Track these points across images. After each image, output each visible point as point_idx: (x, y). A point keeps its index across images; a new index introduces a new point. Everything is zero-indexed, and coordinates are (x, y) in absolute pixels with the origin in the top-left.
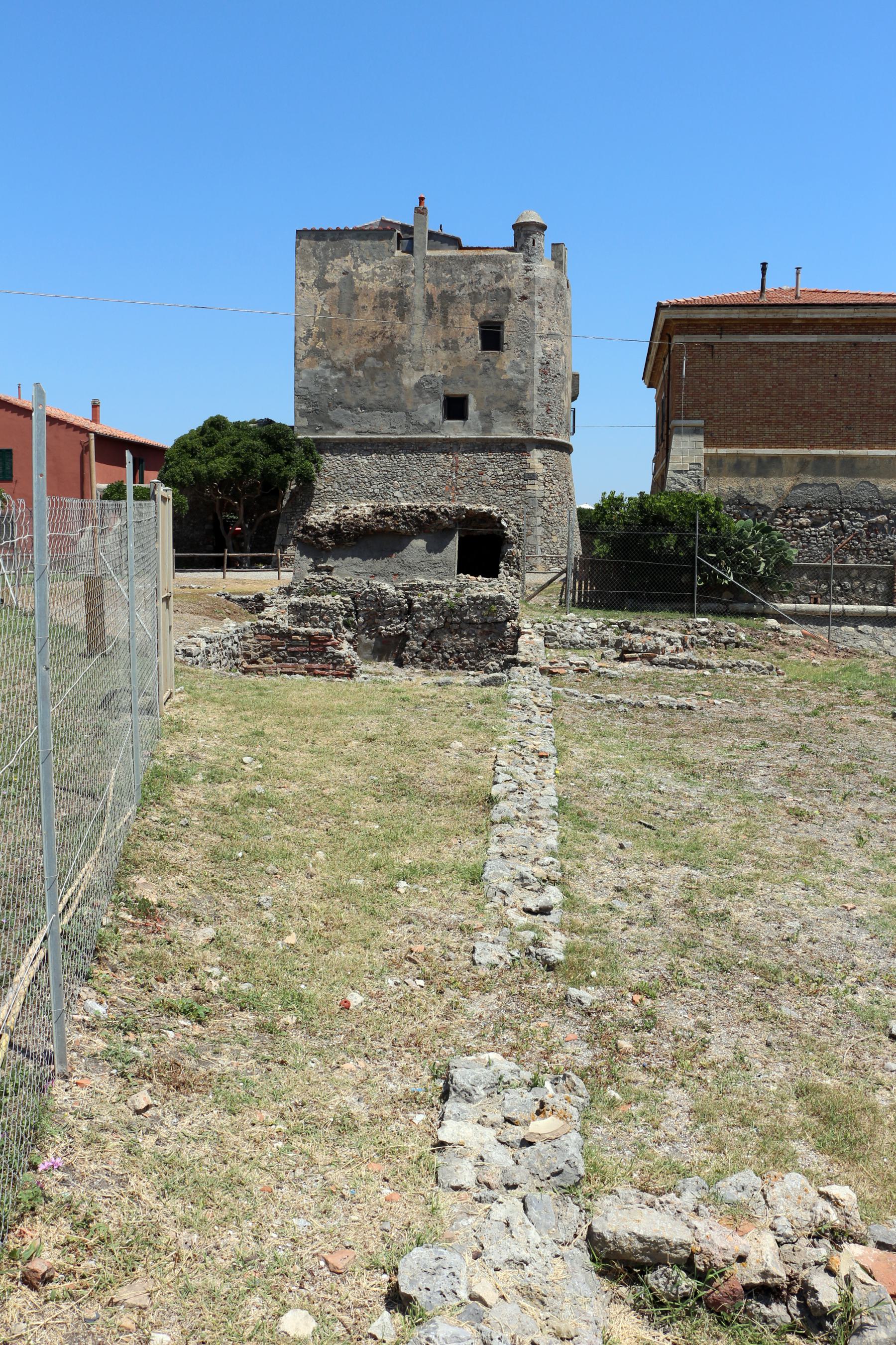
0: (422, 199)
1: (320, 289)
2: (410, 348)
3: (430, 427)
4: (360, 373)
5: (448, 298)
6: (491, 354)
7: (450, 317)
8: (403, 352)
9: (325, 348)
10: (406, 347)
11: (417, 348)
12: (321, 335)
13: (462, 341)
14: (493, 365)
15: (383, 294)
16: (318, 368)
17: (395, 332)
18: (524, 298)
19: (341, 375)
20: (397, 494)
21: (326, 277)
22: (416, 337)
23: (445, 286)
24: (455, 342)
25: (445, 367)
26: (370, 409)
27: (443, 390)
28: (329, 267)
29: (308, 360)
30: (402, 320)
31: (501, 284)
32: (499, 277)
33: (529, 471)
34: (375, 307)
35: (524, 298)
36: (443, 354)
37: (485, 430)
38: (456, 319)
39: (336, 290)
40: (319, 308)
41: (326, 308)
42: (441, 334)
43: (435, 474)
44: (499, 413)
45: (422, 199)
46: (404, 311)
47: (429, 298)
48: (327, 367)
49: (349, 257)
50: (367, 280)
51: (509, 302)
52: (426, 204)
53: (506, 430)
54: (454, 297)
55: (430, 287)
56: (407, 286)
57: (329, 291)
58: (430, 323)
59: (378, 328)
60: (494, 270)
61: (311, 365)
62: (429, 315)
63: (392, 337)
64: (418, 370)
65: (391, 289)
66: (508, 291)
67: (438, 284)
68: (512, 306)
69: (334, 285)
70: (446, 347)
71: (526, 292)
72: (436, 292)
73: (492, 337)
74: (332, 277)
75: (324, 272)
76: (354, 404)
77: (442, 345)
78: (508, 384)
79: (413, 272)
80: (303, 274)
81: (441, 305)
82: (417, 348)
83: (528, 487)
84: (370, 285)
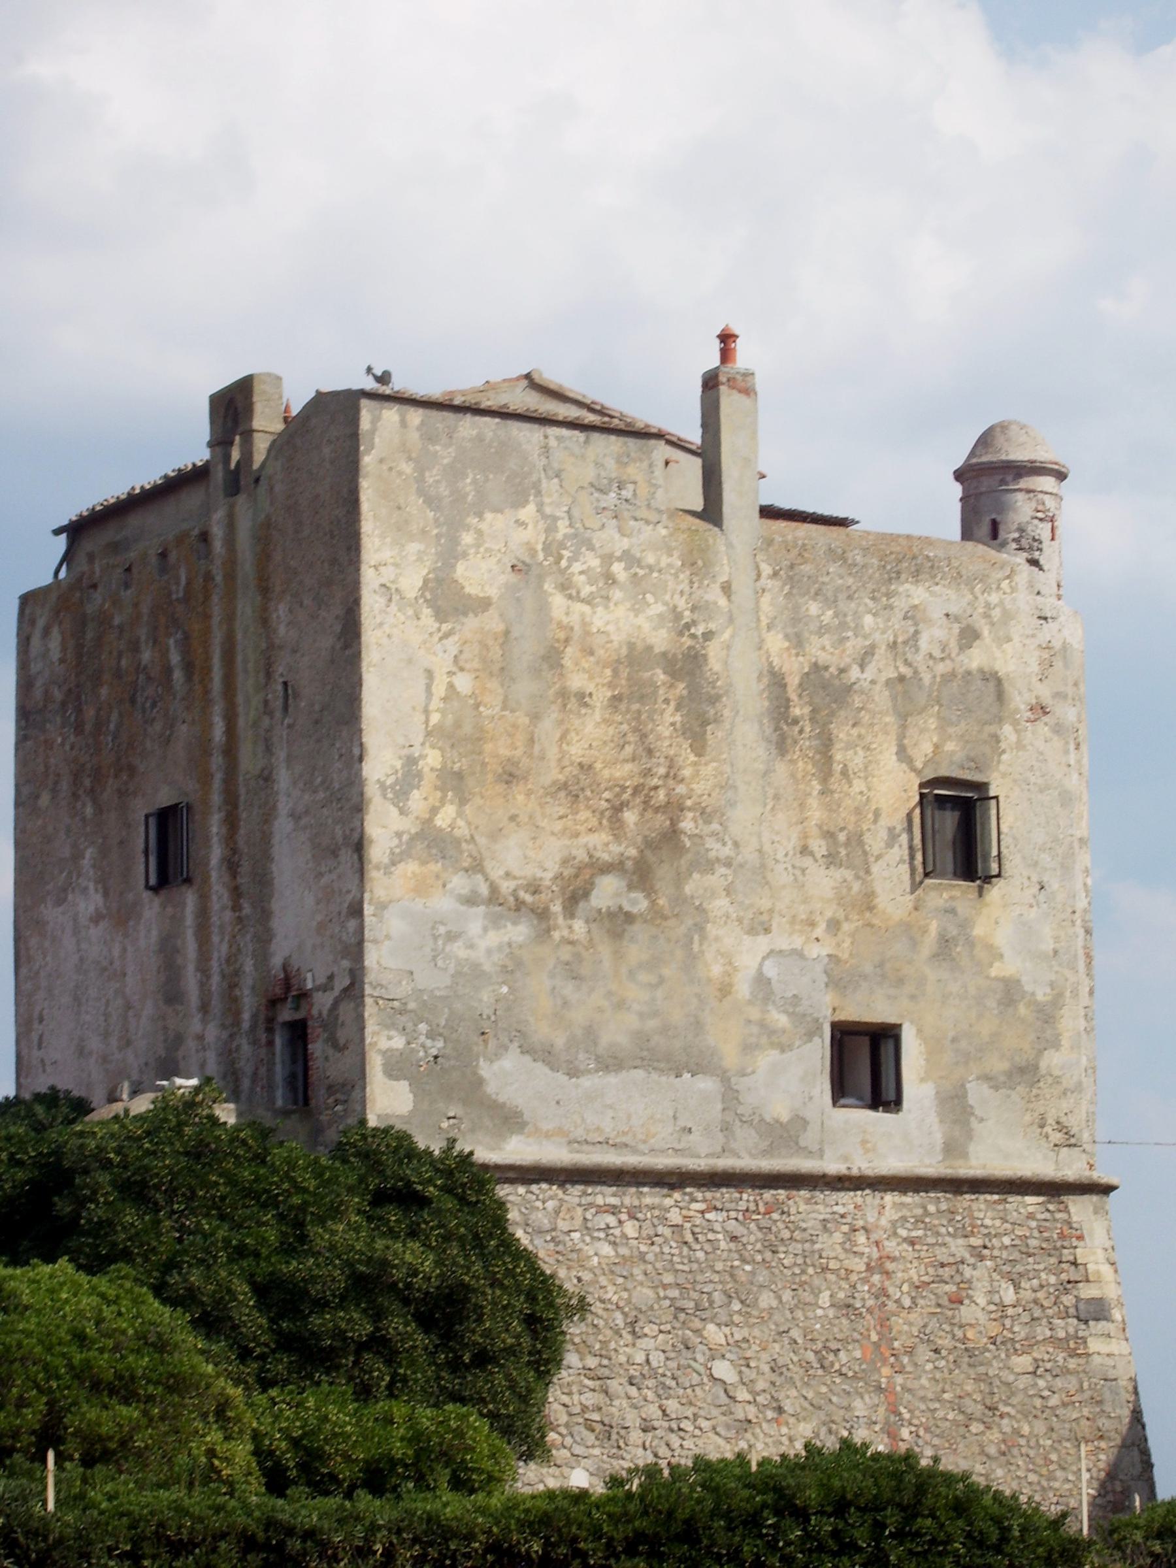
0: (726, 338)
1: (440, 615)
2: (727, 851)
3: (785, 1134)
4: (579, 926)
5: (829, 691)
6: (950, 893)
7: (838, 757)
8: (708, 866)
9: (462, 830)
10: (716, 849)
11: (748, 854)
12: (454, 782)
13: (875, 841)
14: (965, 925)
15: (636, 657)
16: (443, 903)
17: (681, 789)
18: (1041, 710)
19: (519, 932)
20: (723, 1370)
21: (461, 569)
22: (743, 818)
23: (820, 649)
24: (856, 840)
25: (834, 926)
26: (611, 1063)
27: (828, 1007)
28: (467, 538)
29: (411, 867)
30: (699, 747)
31: (975, 659)
32: (969, 636)
33: (1087, 1292)
34: (616, 699)
35: (1041, 710)
36: (824, 882)
37: (952, 1149)
38: (857, 759)
39: (492, 622)
40: (439, 690)
41: (464, 683)
42: (816, 813)
43: (825, 1299)
44: (985, 1088)
45: (726, 338)
46: (705, 723)
47: (777, 681)
48: (471, 900)
49: (528, 512)
50: (588, 601)
51: (1000, 720)
52: (745, 356)
53: (1001, 1150)
54: (849, 689)
55: (776, 642)
56: (708, 636)
57: (471, 623)
58: (781, 769)
59: (624, 772)
60: (953, 609)
61: (421, 888)
62: (782, 746)
63: (674, 808)
64: (752, 931)
65: (661, 639)
66: (995, 682)
67: (797, 642)
68: (1007, 730)
69: (484, 604)
70: (831, 859)
71: (1044, 692)
72: (794, 669)
73: (958, 829)
74: (480, 574)
75: (450, 554)
76: (560, 1041)
77: (819, 846)
78: (1010, 992)
79: (727, 589)
80: (387, 554)
81: (810, 711)
82: (748, 854)
83: (1094, 1345)
84: (599, 619)
